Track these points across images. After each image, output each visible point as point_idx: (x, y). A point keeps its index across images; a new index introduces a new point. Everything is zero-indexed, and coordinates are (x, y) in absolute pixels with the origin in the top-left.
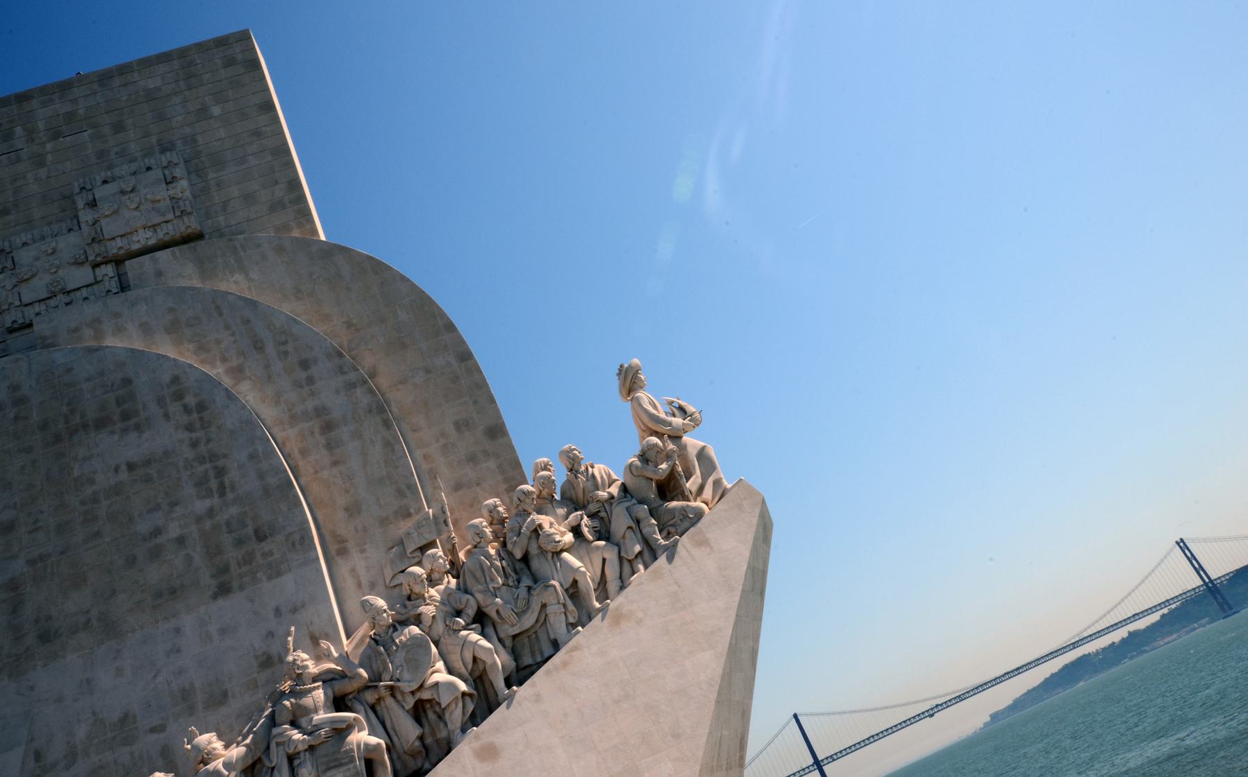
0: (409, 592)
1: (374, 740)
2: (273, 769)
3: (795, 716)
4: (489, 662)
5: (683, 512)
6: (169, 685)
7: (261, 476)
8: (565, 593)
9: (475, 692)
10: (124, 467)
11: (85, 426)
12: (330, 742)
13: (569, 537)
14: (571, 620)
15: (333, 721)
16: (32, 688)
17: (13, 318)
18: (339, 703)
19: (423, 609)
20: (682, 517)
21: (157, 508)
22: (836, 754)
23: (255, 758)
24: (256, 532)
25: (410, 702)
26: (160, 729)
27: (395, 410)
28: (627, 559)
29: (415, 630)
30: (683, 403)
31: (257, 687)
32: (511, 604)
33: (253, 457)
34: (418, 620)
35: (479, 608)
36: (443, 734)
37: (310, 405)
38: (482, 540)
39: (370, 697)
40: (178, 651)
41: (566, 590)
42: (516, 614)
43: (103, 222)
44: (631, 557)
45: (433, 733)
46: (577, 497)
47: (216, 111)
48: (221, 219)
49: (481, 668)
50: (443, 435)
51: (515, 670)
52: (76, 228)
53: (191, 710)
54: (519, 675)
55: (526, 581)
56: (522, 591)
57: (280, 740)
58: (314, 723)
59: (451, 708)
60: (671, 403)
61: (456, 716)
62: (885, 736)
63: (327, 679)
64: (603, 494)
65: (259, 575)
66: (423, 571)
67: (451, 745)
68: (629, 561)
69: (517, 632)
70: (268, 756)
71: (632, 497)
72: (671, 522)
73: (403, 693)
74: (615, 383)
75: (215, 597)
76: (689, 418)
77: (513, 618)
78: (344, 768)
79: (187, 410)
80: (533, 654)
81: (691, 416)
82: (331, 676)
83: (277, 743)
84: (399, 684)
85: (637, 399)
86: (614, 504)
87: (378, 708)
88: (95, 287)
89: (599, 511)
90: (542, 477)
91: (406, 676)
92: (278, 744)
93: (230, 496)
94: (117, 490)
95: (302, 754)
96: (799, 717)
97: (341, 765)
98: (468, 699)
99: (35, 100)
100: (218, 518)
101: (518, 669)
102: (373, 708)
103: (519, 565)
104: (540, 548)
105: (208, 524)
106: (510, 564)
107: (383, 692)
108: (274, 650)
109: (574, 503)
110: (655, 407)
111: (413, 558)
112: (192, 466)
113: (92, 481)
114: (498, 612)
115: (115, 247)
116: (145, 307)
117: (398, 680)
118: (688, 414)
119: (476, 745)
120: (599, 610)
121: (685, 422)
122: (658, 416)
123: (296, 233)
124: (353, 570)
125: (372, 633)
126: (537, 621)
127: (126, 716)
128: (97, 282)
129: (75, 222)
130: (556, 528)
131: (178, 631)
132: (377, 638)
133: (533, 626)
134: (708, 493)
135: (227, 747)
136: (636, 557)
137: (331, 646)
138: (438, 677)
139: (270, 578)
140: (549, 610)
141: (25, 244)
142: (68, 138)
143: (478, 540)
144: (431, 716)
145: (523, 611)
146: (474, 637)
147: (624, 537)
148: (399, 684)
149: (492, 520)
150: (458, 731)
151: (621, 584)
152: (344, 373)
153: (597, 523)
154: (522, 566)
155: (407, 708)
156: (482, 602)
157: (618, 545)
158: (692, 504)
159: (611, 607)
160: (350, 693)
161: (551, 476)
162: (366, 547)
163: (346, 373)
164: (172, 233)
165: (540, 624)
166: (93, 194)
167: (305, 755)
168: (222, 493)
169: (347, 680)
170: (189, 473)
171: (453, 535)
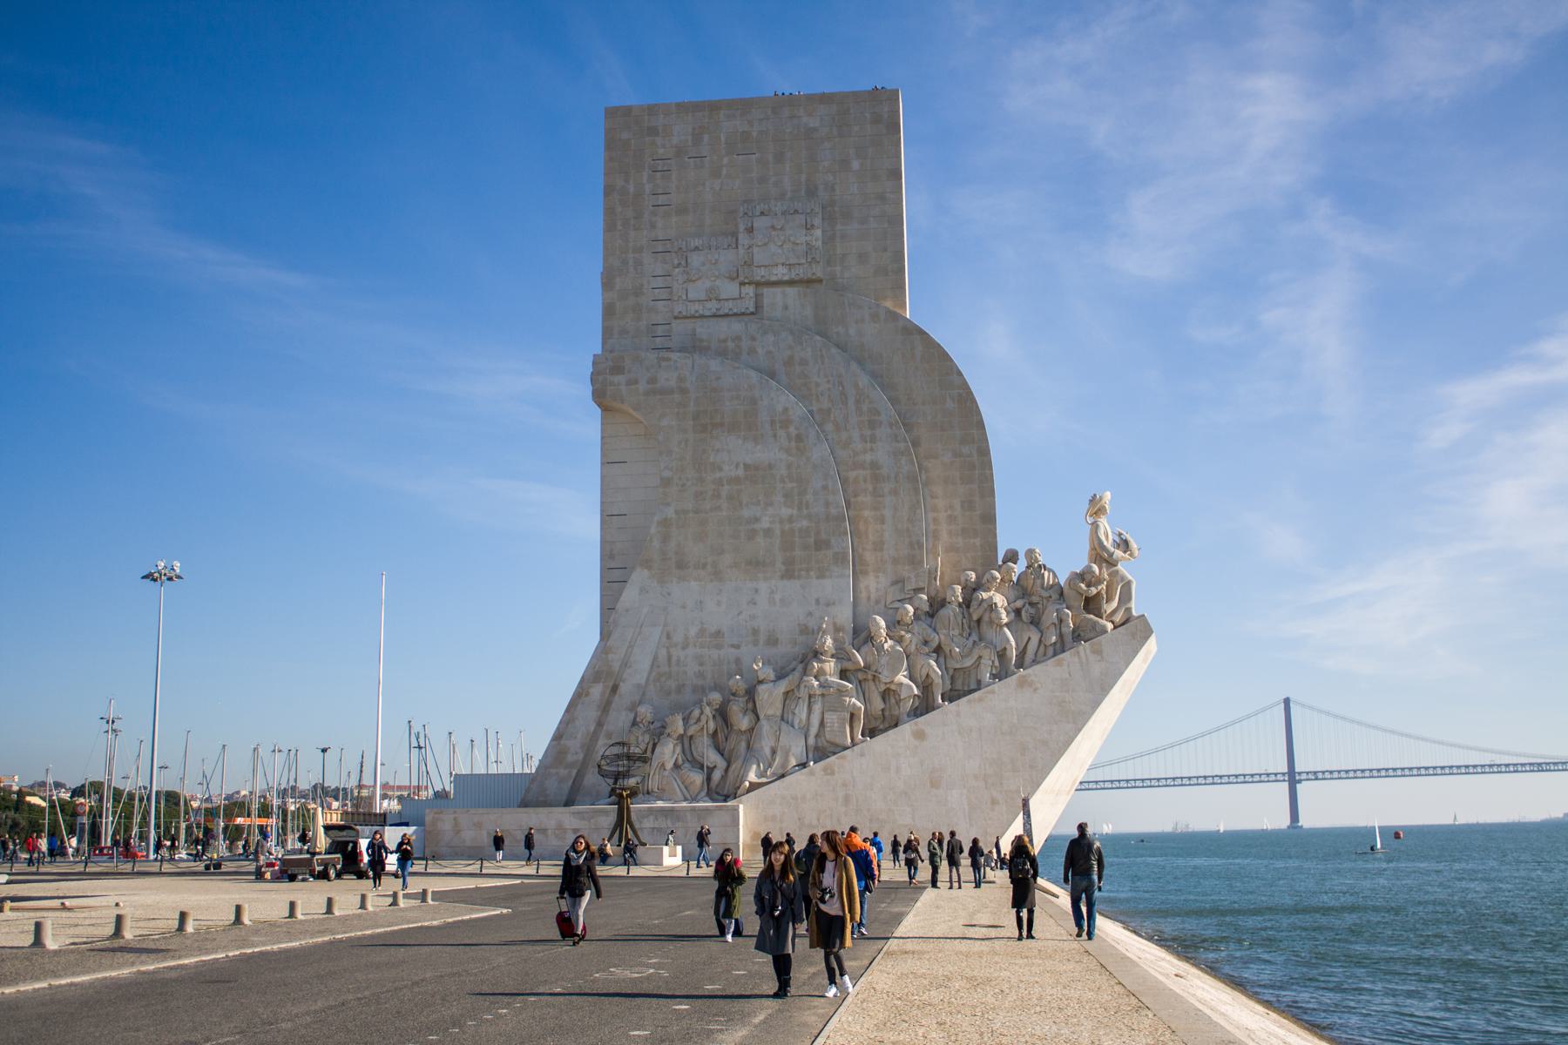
1: (859, 704)
2: (799, 698)
3: (1287, 702)
7: (827, 504)
10: (742, 466)
11: (722, 425)
14: (994, 672)
15: (838, 684)
16: (669, 594)
17: (680, 310)
21: (758, 503)
22: (1323, 772)
24: (816, 542)
25: (883, 688)
26: (737, 647)
27: (924, 477)
33: (825, 488)
36: (896, 713)
39: (861, 676)
40: (755, 604)
43: (756, 250)
44: (1048, 643)
45: (890, 710)
47: (856, 165)
48: (838, 269)
49: (930, 681)
50: (951, 507)
52: (734, 246)
54: (952, 696)
55: (975, 637)
56: (970, 643)
57: (807, 684)
60: (1120, 534)
65: (812, 573)
68: (1045, 646)
69: (958, 666)
70: (798, 690)
73: (879, 681)
75: (782, 577)
78: (839, 713)
79: (789, 439)
80: (963, 684)
84: (880, 676)
86: (1050, 603)
87: (863, 684)
88: (739, 301)
91: (885, 673)
92: (805, 686)
93: (805, 512)
94: (737, 480)
96: (1291, 705)
99: (722, 112)
100: (794, 525)
102: (860, 682)
104: (990, 617)
105: (787, 527)
107: (870, 677)
110: (1107, 537)
112: (784, 482)
113: (721, 469)
114: (950, 651)
115: (760, 274)
116: (773, 338)
123: (889, 304)
124: (867, 587)
126: (972, 665)
128: (741, 298)
129: (734, 240)
131: (756, 591)
136: (1051, 645)
139: (818, 578)
140: (982, 661)
141: (697, 249)
142: (740, 157)
144: (893, 701)
146: (933, 663)
152: (897, 441)
154: (976, 625)
157: (1041, 632)
164: (802, 276)
166: (752, 223)
168: (800, 509)
170: (782, 485)
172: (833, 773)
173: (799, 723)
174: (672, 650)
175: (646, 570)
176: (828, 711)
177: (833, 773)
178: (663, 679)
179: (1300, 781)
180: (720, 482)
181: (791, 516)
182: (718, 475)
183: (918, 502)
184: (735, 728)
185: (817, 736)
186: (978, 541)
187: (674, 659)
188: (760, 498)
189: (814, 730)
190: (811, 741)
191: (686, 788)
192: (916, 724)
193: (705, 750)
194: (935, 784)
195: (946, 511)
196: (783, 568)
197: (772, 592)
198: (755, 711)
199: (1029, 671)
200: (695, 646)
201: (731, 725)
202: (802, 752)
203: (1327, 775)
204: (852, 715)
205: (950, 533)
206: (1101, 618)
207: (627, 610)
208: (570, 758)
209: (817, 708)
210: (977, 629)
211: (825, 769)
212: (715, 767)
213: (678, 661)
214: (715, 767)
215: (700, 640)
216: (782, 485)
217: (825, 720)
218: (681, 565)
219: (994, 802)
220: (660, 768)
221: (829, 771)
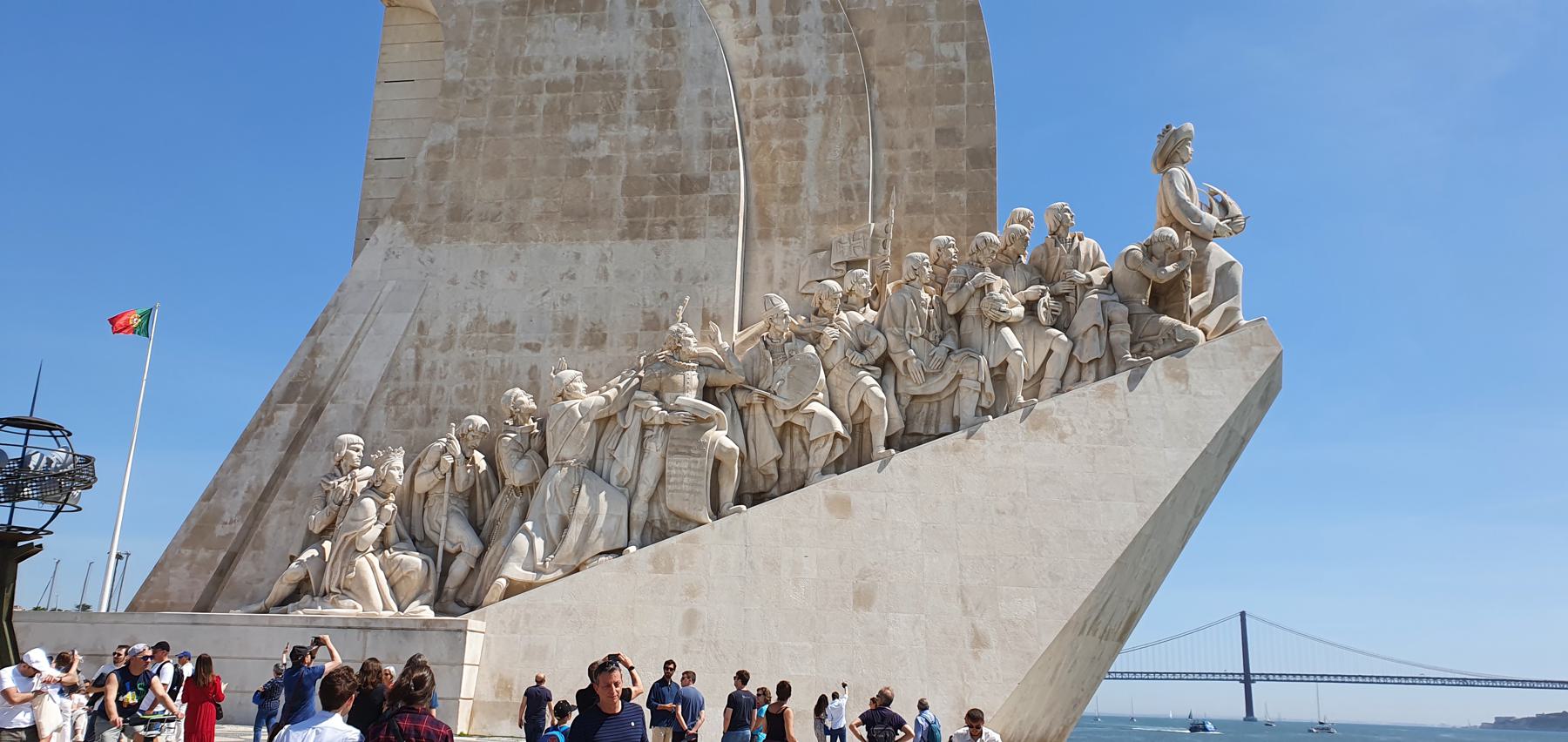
0: (818, 306)
1: (729, 444)
2: (625, 430)
3: (1243, 614)
4: (876, 412)
5: (1171, 332)
6: (555, 308)
7: (708, 120)
8: (988, 371)
9: (850, 438)
10: (574, 62)
12: (685, 428)
13: (1019, 311)
14: (984, 403)
16: (432, 261)
18: (708, 393)
19: (828, 330)
20: (1166, 337)
21: (595, 118)
23: (612, 413)
25: (780, 421)
26: (535, 348)
27: (876, 93)
28: (1078, 361)
29: (810, 349)
30: (1228, 199)
31: (636, 344)
32: (923, 361)
33: (706, 94)
34: (816, 340)
35: (886, 352)
36: (803, 467)
37: (785, 55)
38: (918, 278)
40: (573, 277)
41: (992, 370)
42: (925, 373)
44: (1085, 360)
46: (1048, 267)
50: (920, 140)
51: (901, 433)
53: (567, 341)
54: (901, 440)
55: (950, 342)
56: (941, 351)
58: (677, 402)
59: (819, 443)
60: (1215, 193)
61: (821, 455)
62: (1303, 681)
63: (704, 363)
64: (1081, 276)
65: (673, 229)
66: (840, 289)
67: (807, 482)
68: (1081, 364)
69: (918, 391)
71: (1115, 291)
72: (1150, 338)
74: (1153, 145)
75: (622, 236)
76: (1228, 221)
77: (920, 377)
80: (927, 424)
81: (1232, 218)
82: (709, 362)
83: (636, 406)
85: (1171, 174)
87: (746, 414)
89: (1067, 294)
90: (1013, 229)
91: (784, 393)
92: (636, 408)
93: (670, 132)
95: (656, 428)
96: (1247, 618)
97: (690, 454)
98: (839, 440)
101: (905, 432)
102: (741, 411)
103: (947, 321)
104: (980, 310)
106: (939, 317)
107: (755, 399)
108: (664, 314)
109: (1041, 273)
110: (1190, 190)
111: (836, 270)
113: (539, 68)
114: (905, 363)
117: (775, 394)
118: (1230, 215)
119: (831, 492)
120: (1020, 406)
121: (1221, 223)
122: (1190, 205)
124: (769, 261)
125: (765, 334)
127: (508, 322)
130: (1008, 296)
131: (578, 256)
132: (768, 341)
133: (938, 394)
134: (1211, 321)
135: (588, 391)
137: (719, 332)
138: (815, 406)
140: (963, 383)
143: (913, 277)
145: (933, 373)
146: (869, 380)
147: (1085, 334)
148: (774, 397)
149: (937, 260)
150: (819, 470)
151: (1060, 387)
153: (1059, 307)
154: (953, 323)
155: (774, 426)
156: (892, 346)
158: (1187, 327)
159: (1036, 407)
160: (723, 387)
161: (1026, 233)
162: (790, 239)
163: (836, 31)
165: (946, 394)
167: (658, 430)
169: (724, 371)
171: (888, 261)
172: (669, 569)
173: (621, 473)
174: (425, 352)
175: (399, 223)
176: (672, 454)
177: (669, 569)
178: (403, 400)
179: (1254, 681)
180: (535, 88)
181: (647, 139)
182: (534, 76)
183: (863, 126)
184: (507, 483)
185: (652, 500)
186: (963, 195)
187: (426, 366)
188: (599, 112)
189: (644, 490)
190: (640, 508)
191: (392, 588)
192: (834, 485)
193: (444, 520)
194: (863, 599)
195: (911, 146)
196: (626, 220)
197: (604, 259)
198: (543, 452)
199: (1051, 403)
200: (464, 345)
201: (504, 479)
202: (618, 528)
203: (1277, 678)
204: (717, 464)
205: (916, 181)
206: (1185, 321)
207: (361, 286)
208: (220, 531)
209: (655, 448)
210: (954, 330)
211: (655, 561)
212: (459, 552)
213: (432, 371)
214: (459, 552)
215: (474, 335)
216: (636, 91)
217: (667, 471)
218: (457, 215)
219: (979, 641)
220: (346, 551)
221: (662, 566)
